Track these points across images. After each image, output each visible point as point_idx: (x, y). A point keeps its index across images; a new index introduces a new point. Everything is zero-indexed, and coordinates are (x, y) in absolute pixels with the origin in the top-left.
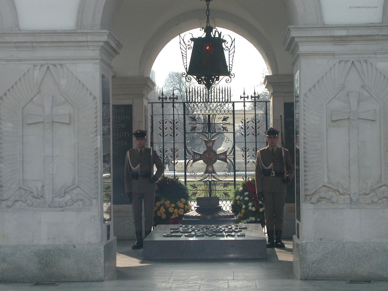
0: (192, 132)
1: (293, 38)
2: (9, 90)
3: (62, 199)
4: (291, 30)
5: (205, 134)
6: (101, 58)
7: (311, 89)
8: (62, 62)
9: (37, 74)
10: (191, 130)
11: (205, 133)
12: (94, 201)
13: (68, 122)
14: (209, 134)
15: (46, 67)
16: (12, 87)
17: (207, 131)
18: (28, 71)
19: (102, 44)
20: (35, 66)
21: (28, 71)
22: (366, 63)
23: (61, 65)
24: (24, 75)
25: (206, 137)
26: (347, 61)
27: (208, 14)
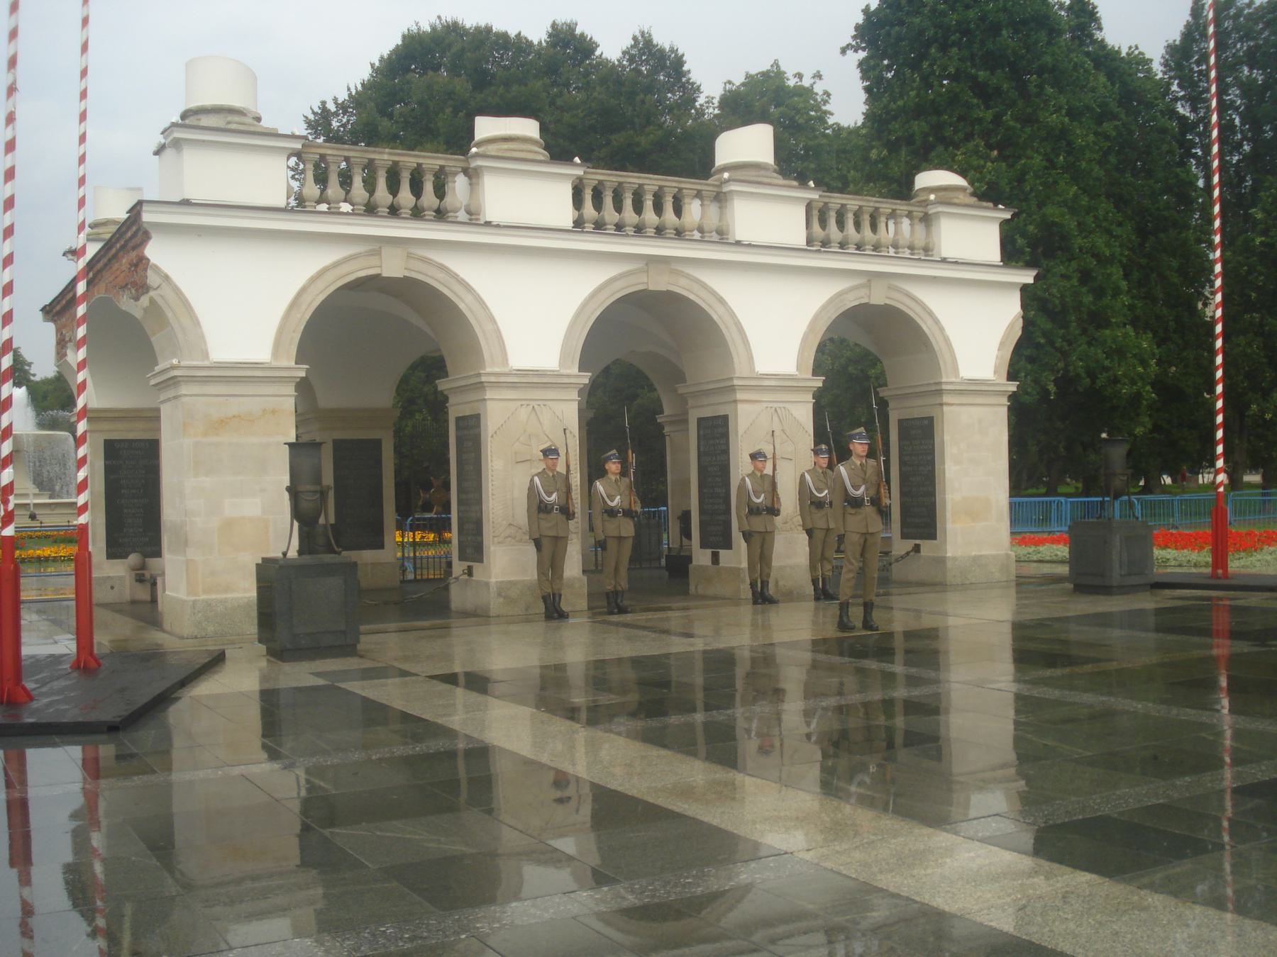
9: (524, 413)
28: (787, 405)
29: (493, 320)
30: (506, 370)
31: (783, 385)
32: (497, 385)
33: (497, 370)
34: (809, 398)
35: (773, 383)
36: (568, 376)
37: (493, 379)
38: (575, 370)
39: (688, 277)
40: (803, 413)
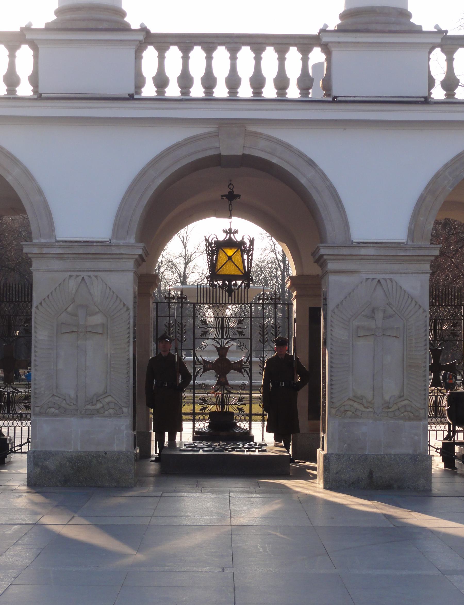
0: (202, 337)
1: (322, 256)
2: (44, 299)
3: (94, 407)
4: (320, 248)
5: (217, 340)
6: (134, 270)
7: (338, 305)
8: (96, 274)
9: (72, 285)
10: (201, 335)
11: (218, 338)
12: (125, 410)
13: (101, 332)
14: (223, 340)
15: (80, 278)
16: (48, 296)
17: (220, 337)
18: (64, 281)
19: (137, 257)
20: (71, 276)
21: (64, 281)
22: (392, 282)
23: (96, 277)
24: (59, 285)
25: (219, 343)
26: (373, 279)
27: (231, 209)
28: (396, 278)
29: (40, 192)
30: (53, 241)
31: (387, 252)
32: (42, 256)
33: (43, 241)
34: (427, 267)
35: (372, 252)
36: (118, 246)
37: (36, 250)
38: (132, 240)
39: (269, 139)
40: (416, 284)
